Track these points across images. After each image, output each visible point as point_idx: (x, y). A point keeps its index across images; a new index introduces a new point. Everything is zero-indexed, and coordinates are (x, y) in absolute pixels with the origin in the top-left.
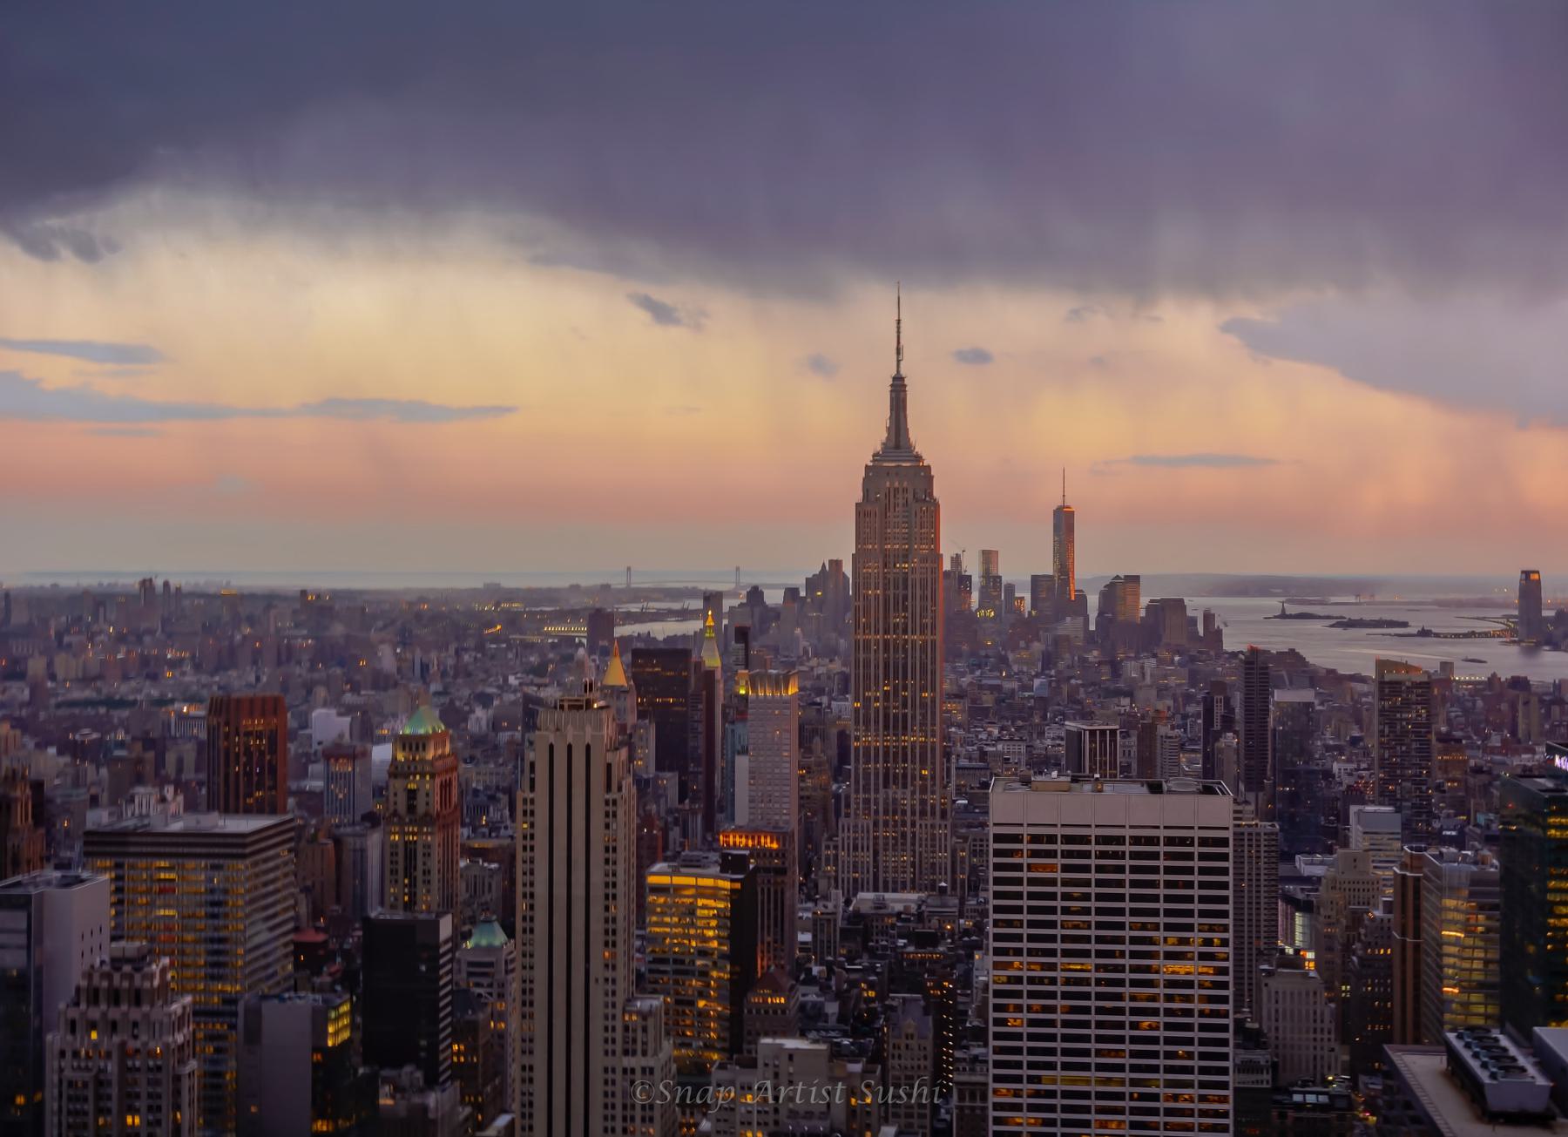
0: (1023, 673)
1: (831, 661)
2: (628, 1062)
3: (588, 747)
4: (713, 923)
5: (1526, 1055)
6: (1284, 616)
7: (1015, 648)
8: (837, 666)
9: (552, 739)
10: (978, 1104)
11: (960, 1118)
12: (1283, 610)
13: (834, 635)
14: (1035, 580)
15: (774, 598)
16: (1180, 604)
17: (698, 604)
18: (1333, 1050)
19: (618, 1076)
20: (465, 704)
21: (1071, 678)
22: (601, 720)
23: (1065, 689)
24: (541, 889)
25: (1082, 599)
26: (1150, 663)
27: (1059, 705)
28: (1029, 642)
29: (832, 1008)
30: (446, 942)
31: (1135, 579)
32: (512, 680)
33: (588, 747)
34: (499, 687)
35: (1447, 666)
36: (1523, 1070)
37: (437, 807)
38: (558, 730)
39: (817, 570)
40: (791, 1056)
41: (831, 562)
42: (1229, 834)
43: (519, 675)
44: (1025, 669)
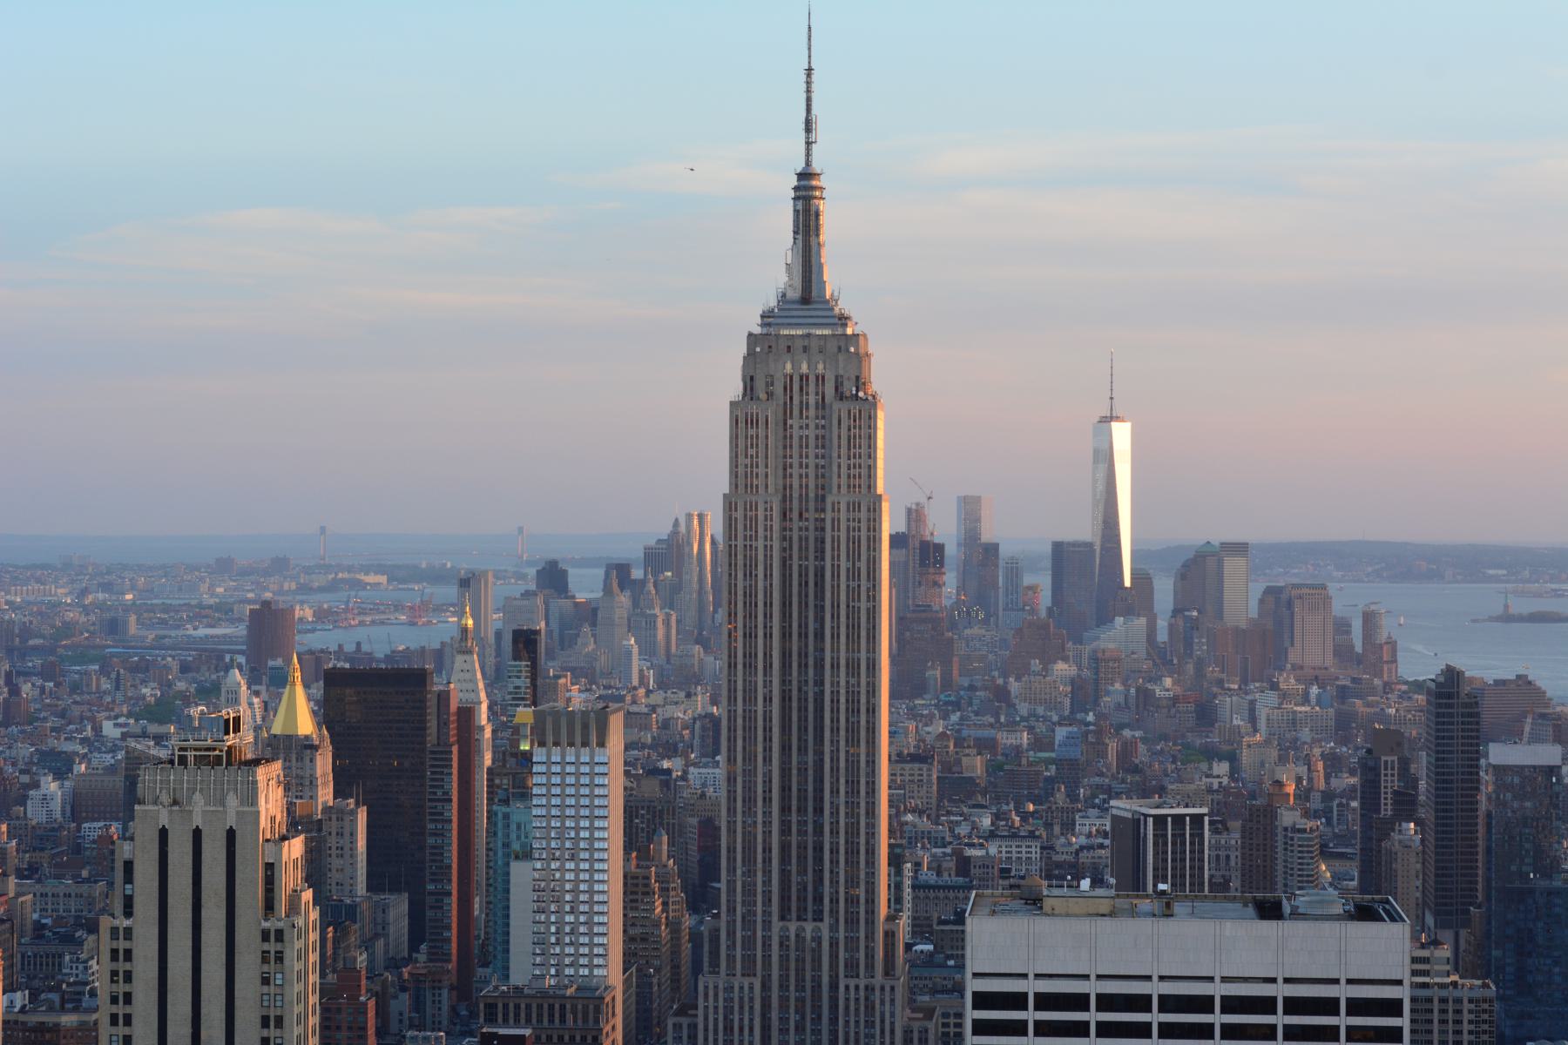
0: (1037, 717)
1: (688, 695)
6: (1507, 618)
7: (1021, 672)
8: (701, 703)
12: (1506, 606)
13: (697, 649)
14: (1060, 551)
15: (586, 586)
16: (1318, 596)
17: (451, 592)
20: (22, 772)
21: (1121, 727)
23: (1112, 747)
26: (1267, 702)
27: (1101, 774)
28: (1047, 663)
31: (1240, 549)
32: (110, 730)
34: (84, 741)
39: (668, 529)
41: (689, 516)
43: (122, 720)
44: (1040, 710)
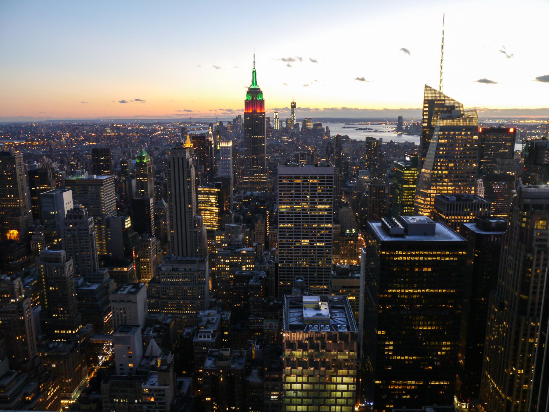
2: (196, 230)
3: (183, 158)
4: (214, 199)
5: (399, 222)
6: (344, 128)
9: (174, 156)
10: (275, 237)
11: (271, 241)
15: (225, 124)
16: (320, 125)
17: (207, 126)
18: (354, 224)
19: (193, 233)
22: (185, 151)
24: (173, 191)
25: (298, 124)
26: (314, 139)
29: (242, 217)
30: (152, 204)
33: (183, 158)
35: (381, 139)
36: (398, 225)
37: (148, 173)
38: (175, 154)
40: (233, 228)
42: (333, 176)
